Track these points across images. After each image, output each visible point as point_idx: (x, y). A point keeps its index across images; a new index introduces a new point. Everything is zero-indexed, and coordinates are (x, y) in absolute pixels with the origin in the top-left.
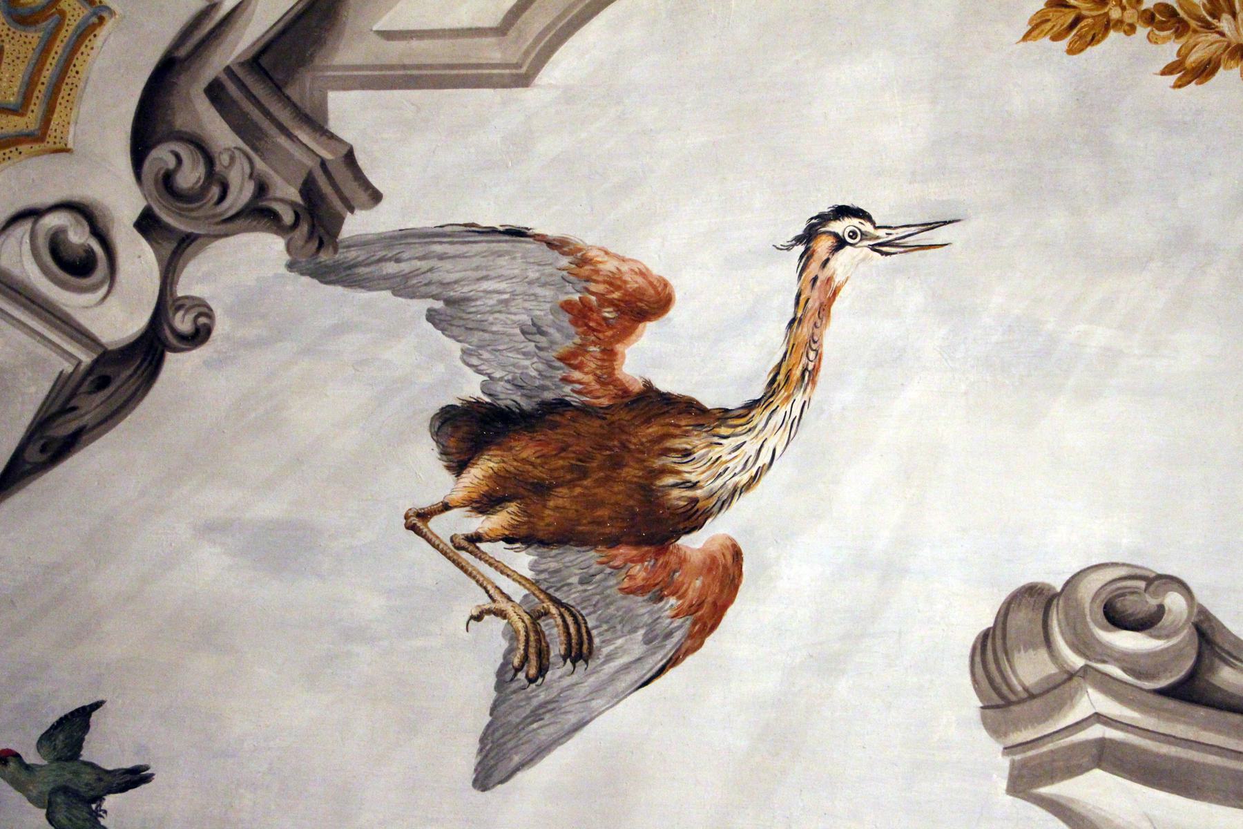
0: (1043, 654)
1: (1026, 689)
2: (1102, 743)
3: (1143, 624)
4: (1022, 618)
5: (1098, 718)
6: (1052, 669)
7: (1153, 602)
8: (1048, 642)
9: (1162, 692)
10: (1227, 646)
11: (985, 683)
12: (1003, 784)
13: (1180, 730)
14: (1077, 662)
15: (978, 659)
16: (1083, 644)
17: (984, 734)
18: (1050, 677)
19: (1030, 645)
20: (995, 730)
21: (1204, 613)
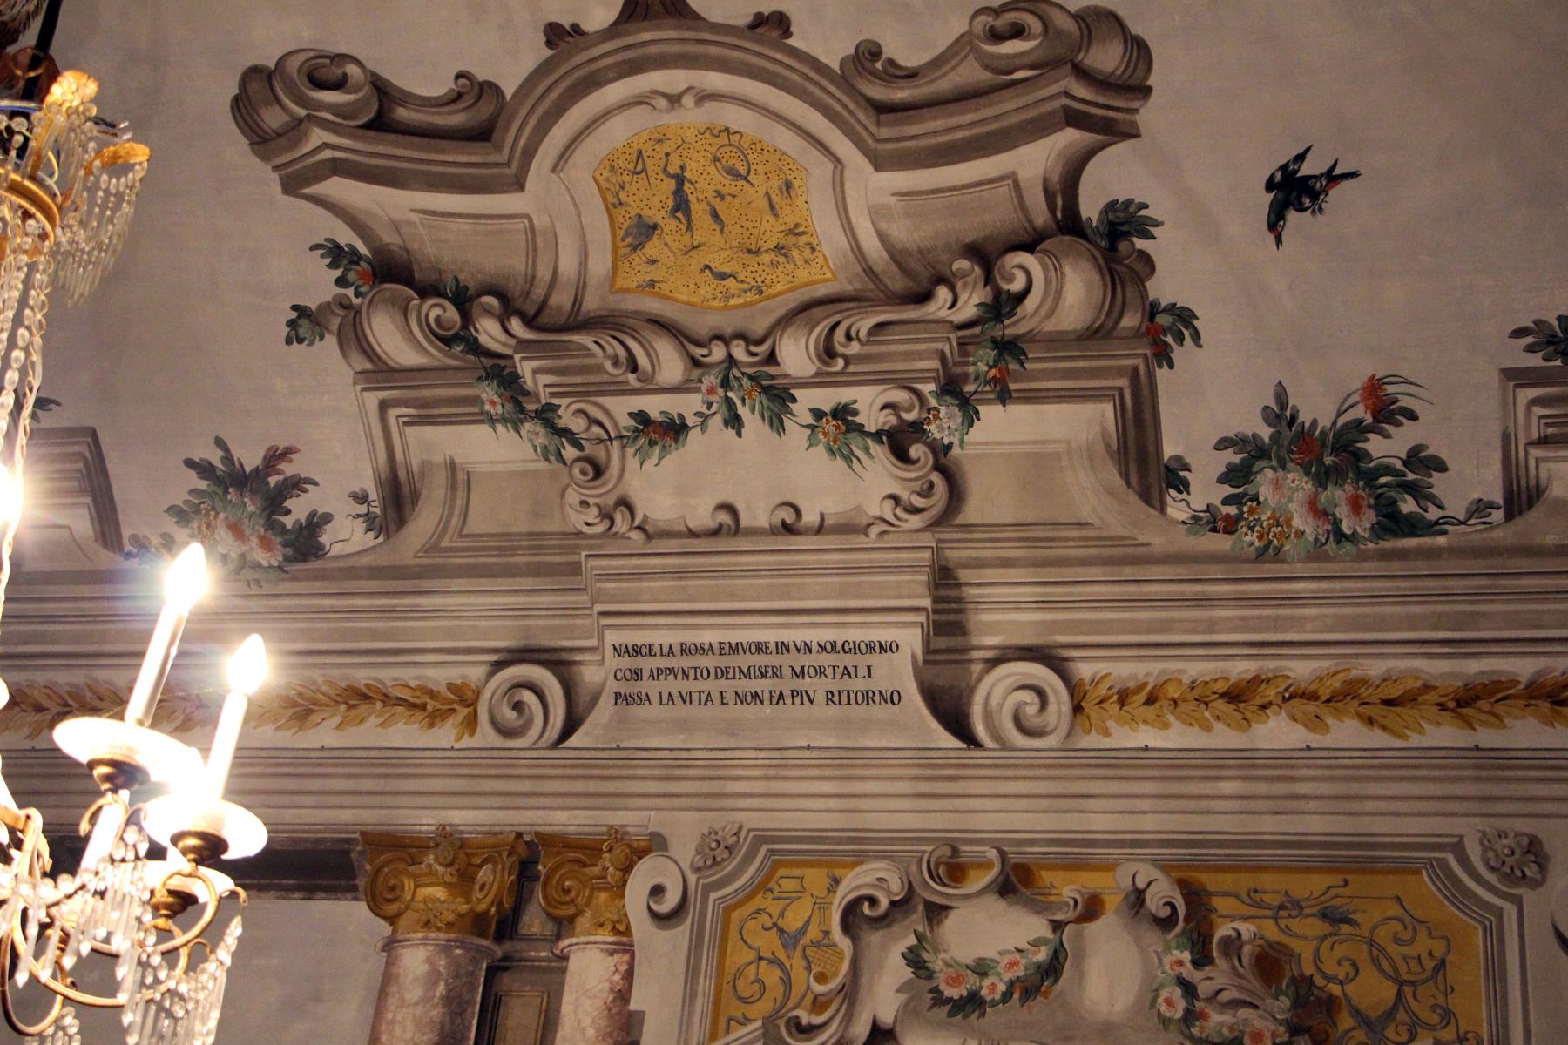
0: (277, 109)
1: (273, 131)
2: (333, 160)
3: (339, 84)
4: (254, 87)
5: (326, 146)
6: (286, 118)
7: (339, 71)
8: (278, 101)
9: (365, 127)
10: (397, 95)
11: (246, 128)
12: (279, 189)
13: (381, 149)
14: (302, 112)
15: (237, 114)
16: (302, 101)
17: (257, 161)
18: (286, 123)
19: (267, 104)
20: (264, 157)
21: (373, 74)
